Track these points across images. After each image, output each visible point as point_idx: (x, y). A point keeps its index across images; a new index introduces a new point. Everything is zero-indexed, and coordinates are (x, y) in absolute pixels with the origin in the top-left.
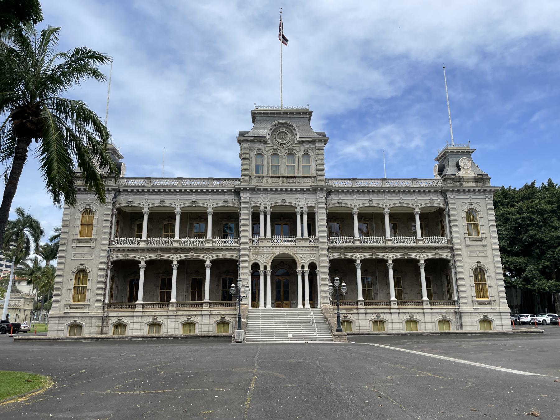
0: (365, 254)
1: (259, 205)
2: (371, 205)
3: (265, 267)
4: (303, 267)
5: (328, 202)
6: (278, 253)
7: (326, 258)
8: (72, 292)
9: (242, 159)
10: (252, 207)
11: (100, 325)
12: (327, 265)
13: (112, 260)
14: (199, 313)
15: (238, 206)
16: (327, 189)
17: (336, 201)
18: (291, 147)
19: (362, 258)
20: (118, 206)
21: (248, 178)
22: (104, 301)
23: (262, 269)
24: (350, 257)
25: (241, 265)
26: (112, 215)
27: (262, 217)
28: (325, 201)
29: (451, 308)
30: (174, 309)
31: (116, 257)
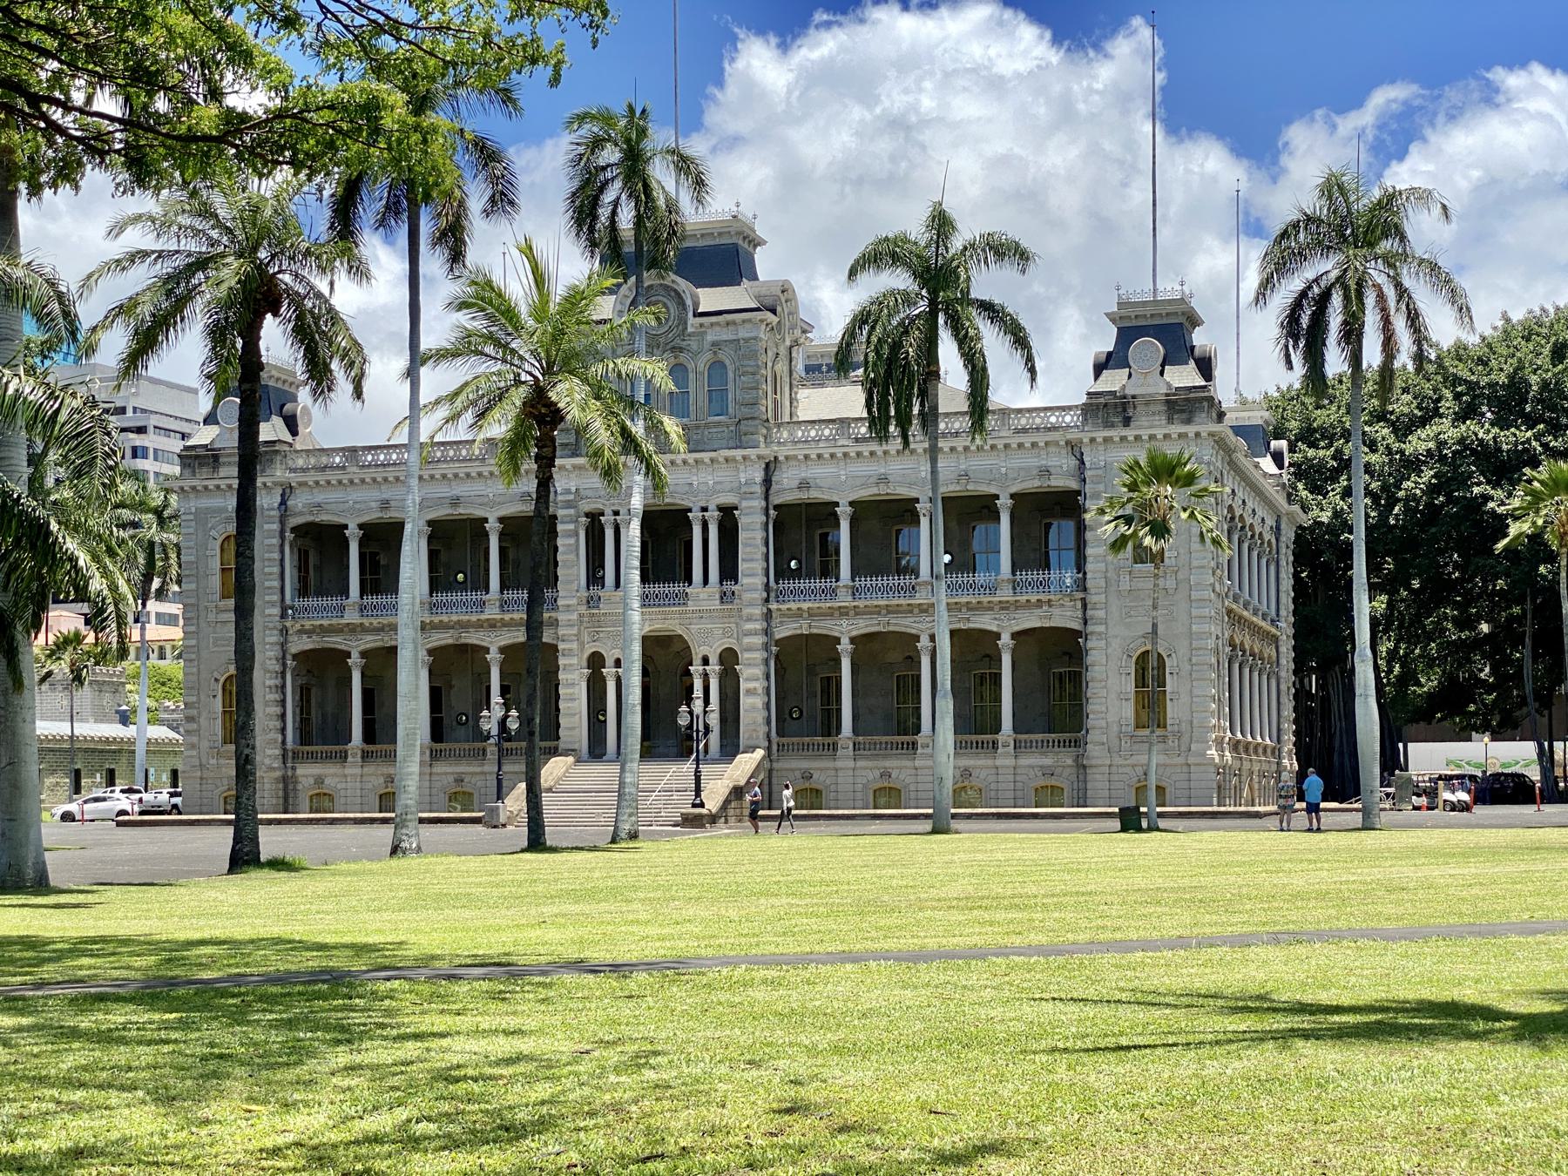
2: (883, 489)
4: (706, 661)
5: (774, 487)
8: (219, 721)
11: (281, 793)
12: (759, 655)
14: (478, 769)
19: (854, 633)
20: (294, 521)
22: (284, 742)
24: (824, 632)
25: (562, 661)
26: (282, 546)
28: (759, 489)
29: (1066, 758)
31: (299, 644)
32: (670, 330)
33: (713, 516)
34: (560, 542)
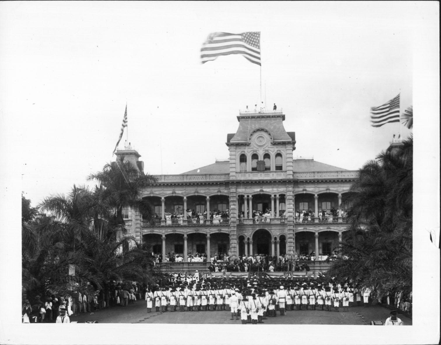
0: (322, 228)
1: (243, 194)
2: (328, 191)
3: (248, 239)
4: (275, 238)
6: (258, 229)
7: (291, 232)
9: (230, 151)
10: (239, 196)
13: (144, 234)
15: (227, 195)
16: (293, 181)
17: (301, 189)
18: (267, 148)
21: (234, 174)
23: (246, 240)
27: (246, 202)
30: (187, 266)
32: (264, 145)
33: (278, 196)
34: (231, 204)
